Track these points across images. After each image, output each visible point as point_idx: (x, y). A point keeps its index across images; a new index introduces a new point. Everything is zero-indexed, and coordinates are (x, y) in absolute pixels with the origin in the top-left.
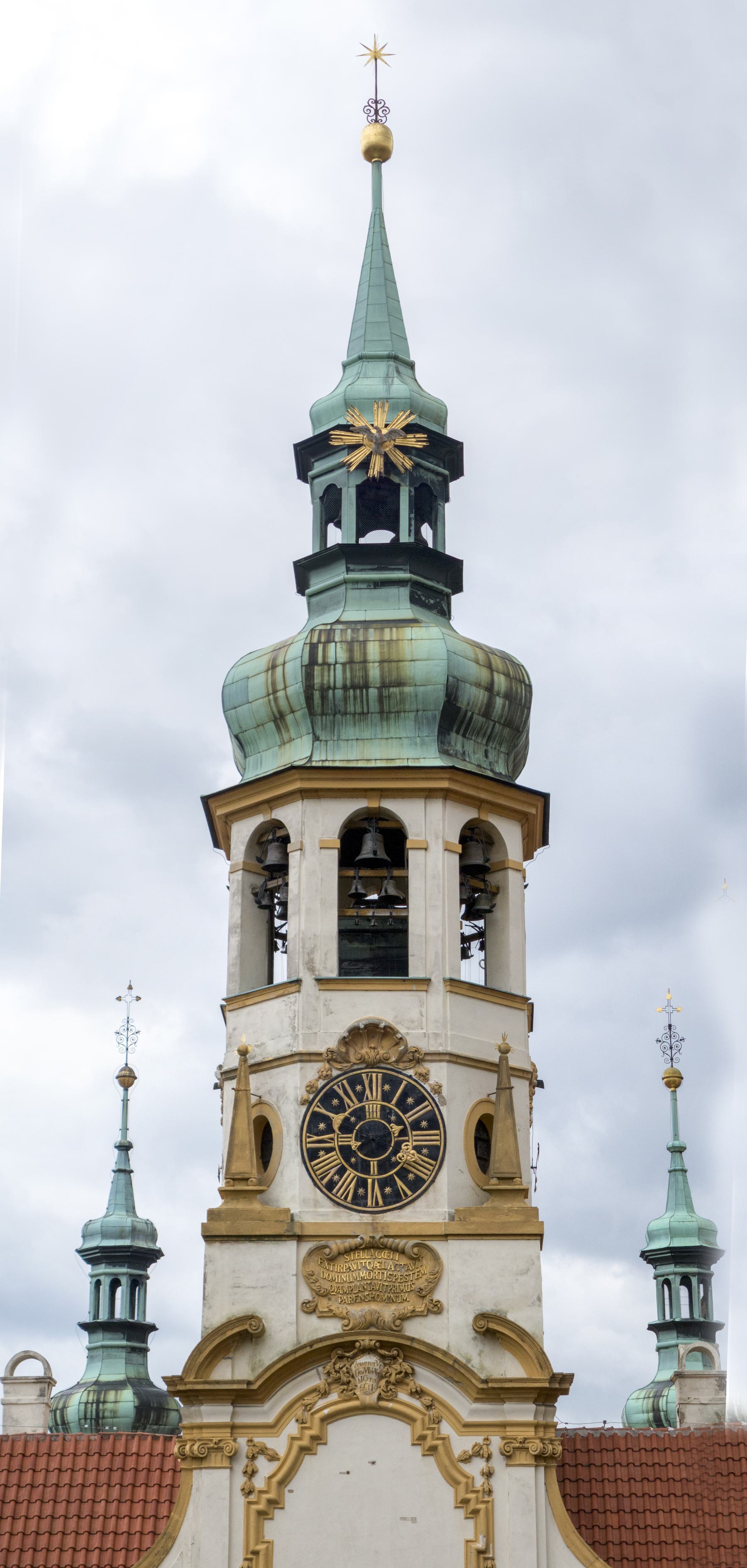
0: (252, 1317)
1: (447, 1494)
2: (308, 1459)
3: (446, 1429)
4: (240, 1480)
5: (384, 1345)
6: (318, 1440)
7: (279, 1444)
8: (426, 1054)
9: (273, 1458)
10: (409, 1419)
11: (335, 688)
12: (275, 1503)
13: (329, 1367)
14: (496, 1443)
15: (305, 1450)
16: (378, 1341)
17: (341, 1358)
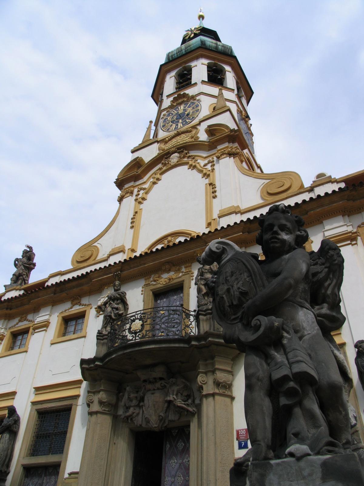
0: (138, 157)
1: (200, 175)
2: (156, 186)
3: (199, 161)
4: (134, 197)
5: (178, 149)
6: (158, 179)
7: (146, 186)
8: (195, 95)
9: (144, 189)
10: (186, 163)
11: (174, 54)
12: (144, 199)
13: (163, 162)
14: (215, 158)
15: (154, 183)
16: (176, 148)
17: (166, 158)
